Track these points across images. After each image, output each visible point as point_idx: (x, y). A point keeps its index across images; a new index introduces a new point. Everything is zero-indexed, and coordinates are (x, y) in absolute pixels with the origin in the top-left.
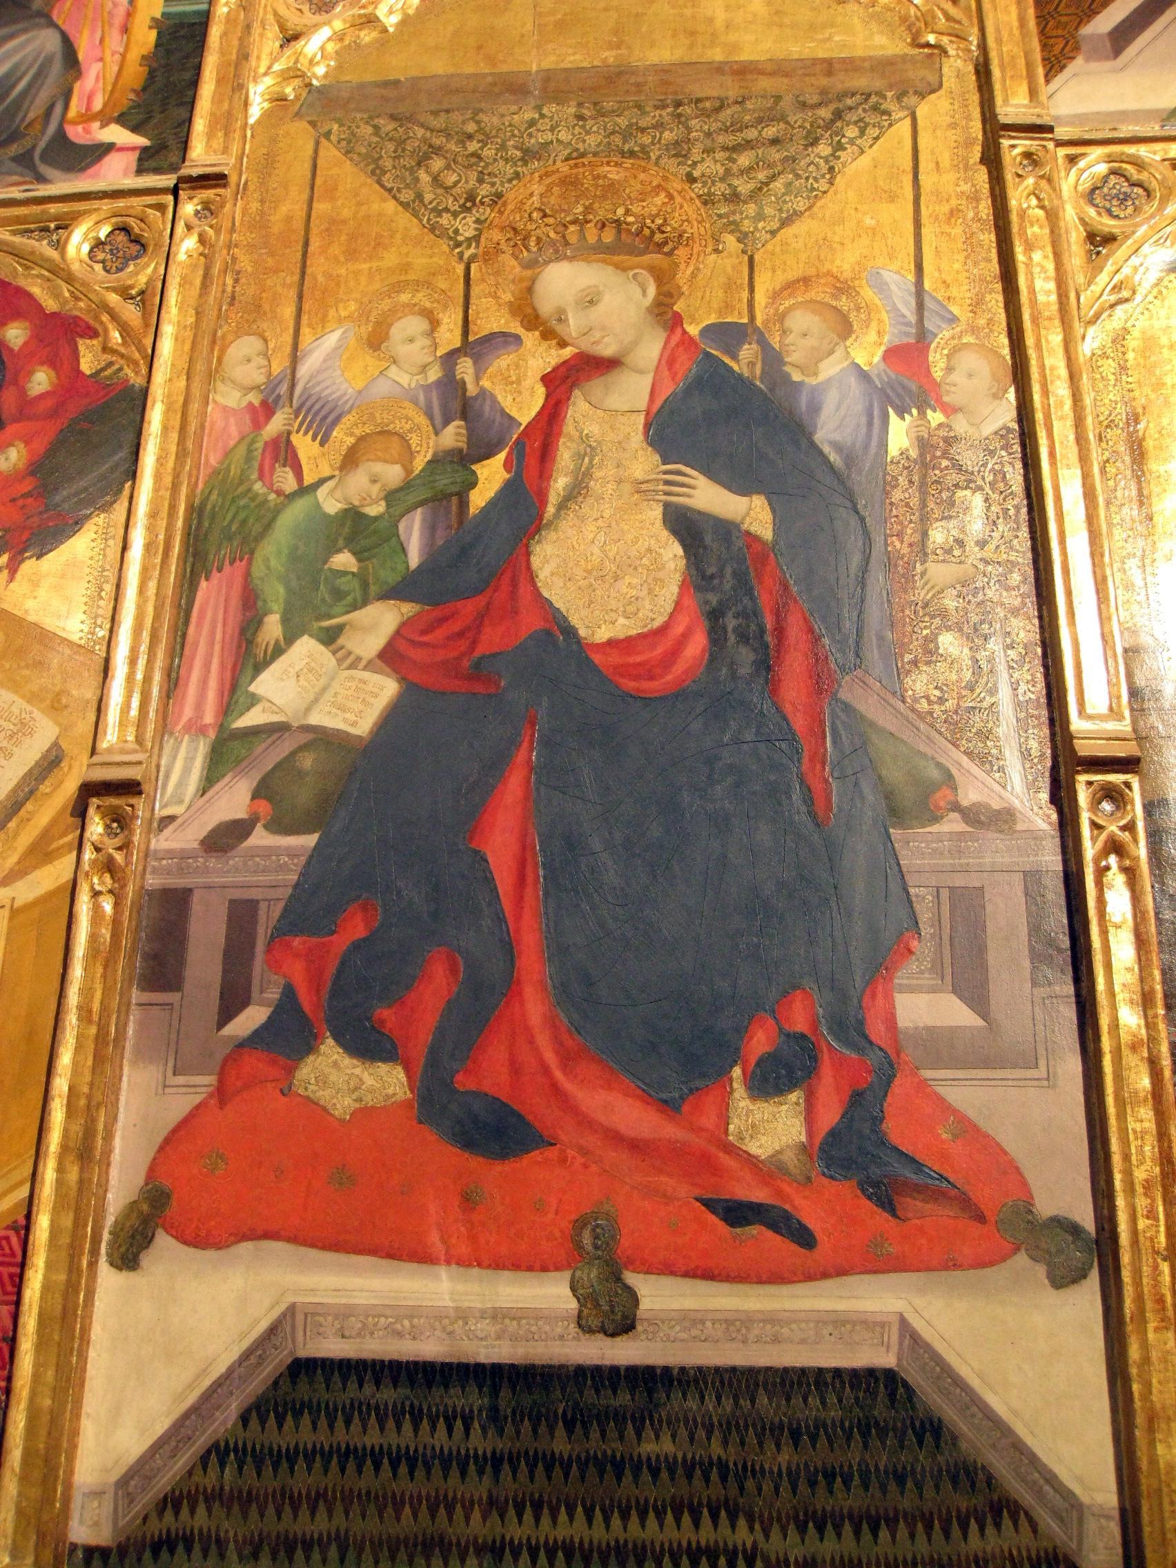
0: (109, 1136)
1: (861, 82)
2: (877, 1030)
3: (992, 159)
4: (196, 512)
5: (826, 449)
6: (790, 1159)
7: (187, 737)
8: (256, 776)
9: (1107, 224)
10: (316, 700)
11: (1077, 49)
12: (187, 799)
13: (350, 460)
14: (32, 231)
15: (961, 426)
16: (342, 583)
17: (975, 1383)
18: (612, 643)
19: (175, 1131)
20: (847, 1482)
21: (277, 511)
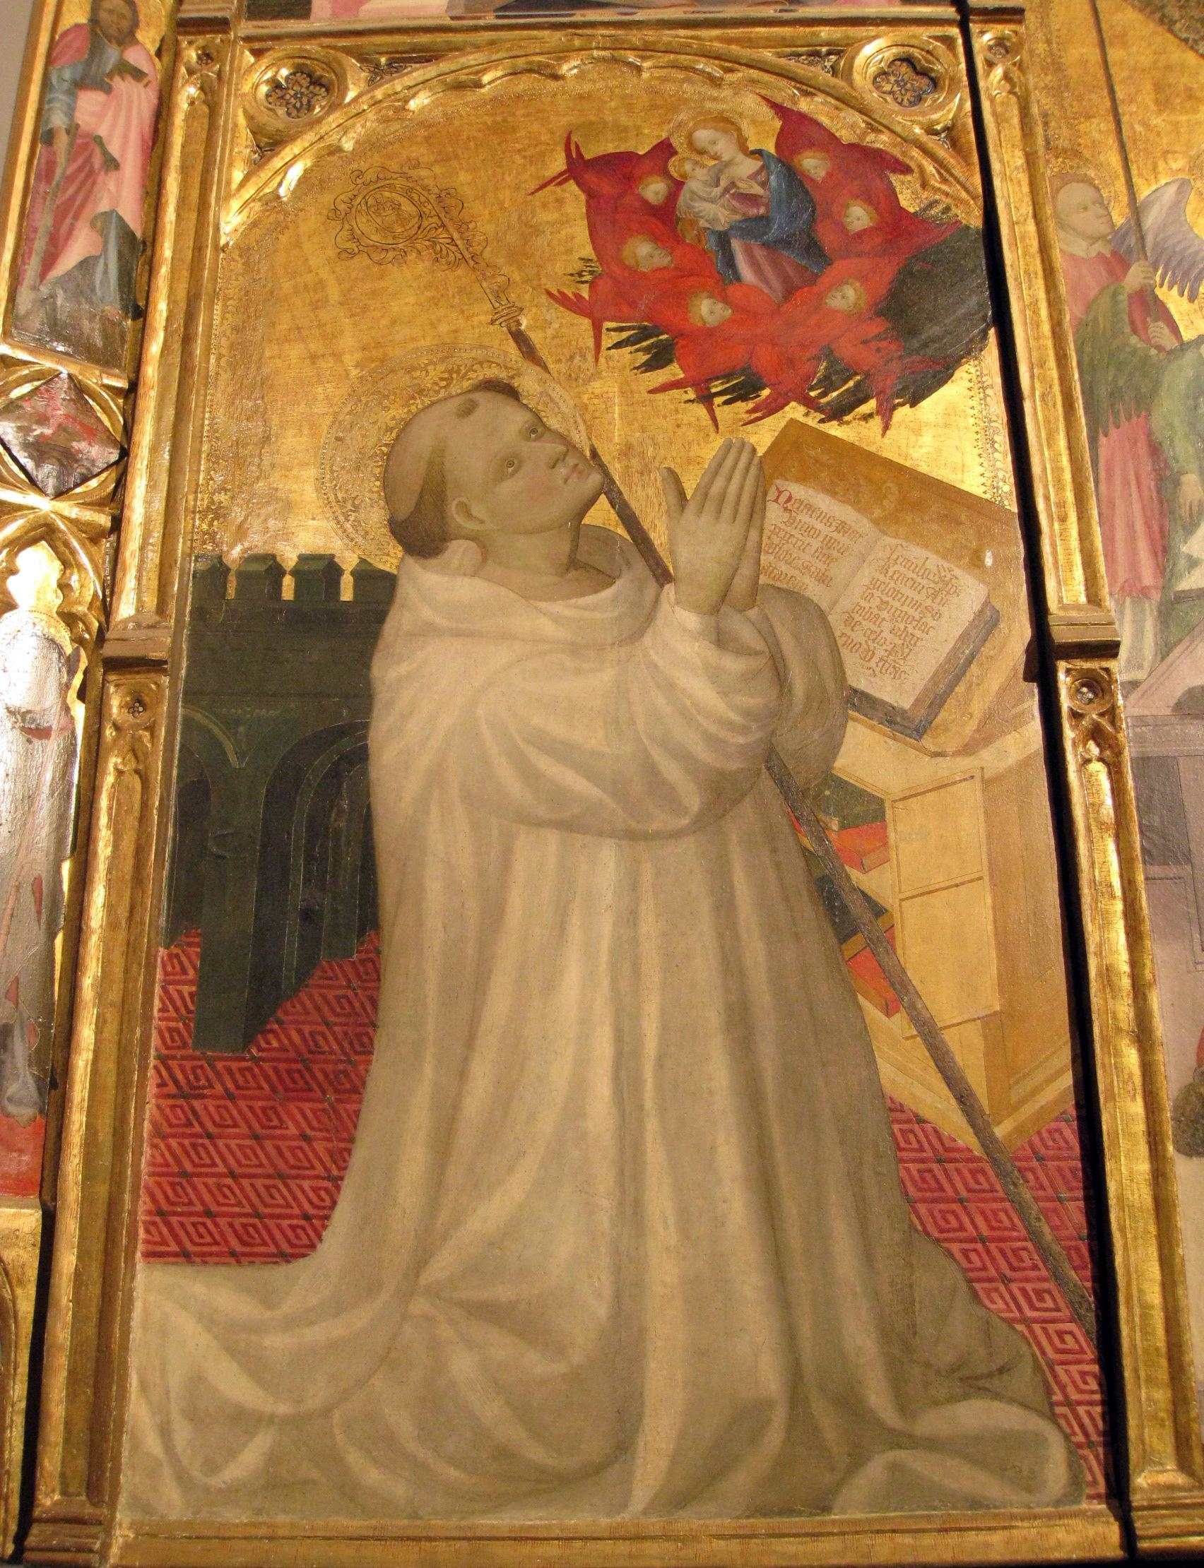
7: (1128, 600)
12: (1147, 665)
14: (800, 55)
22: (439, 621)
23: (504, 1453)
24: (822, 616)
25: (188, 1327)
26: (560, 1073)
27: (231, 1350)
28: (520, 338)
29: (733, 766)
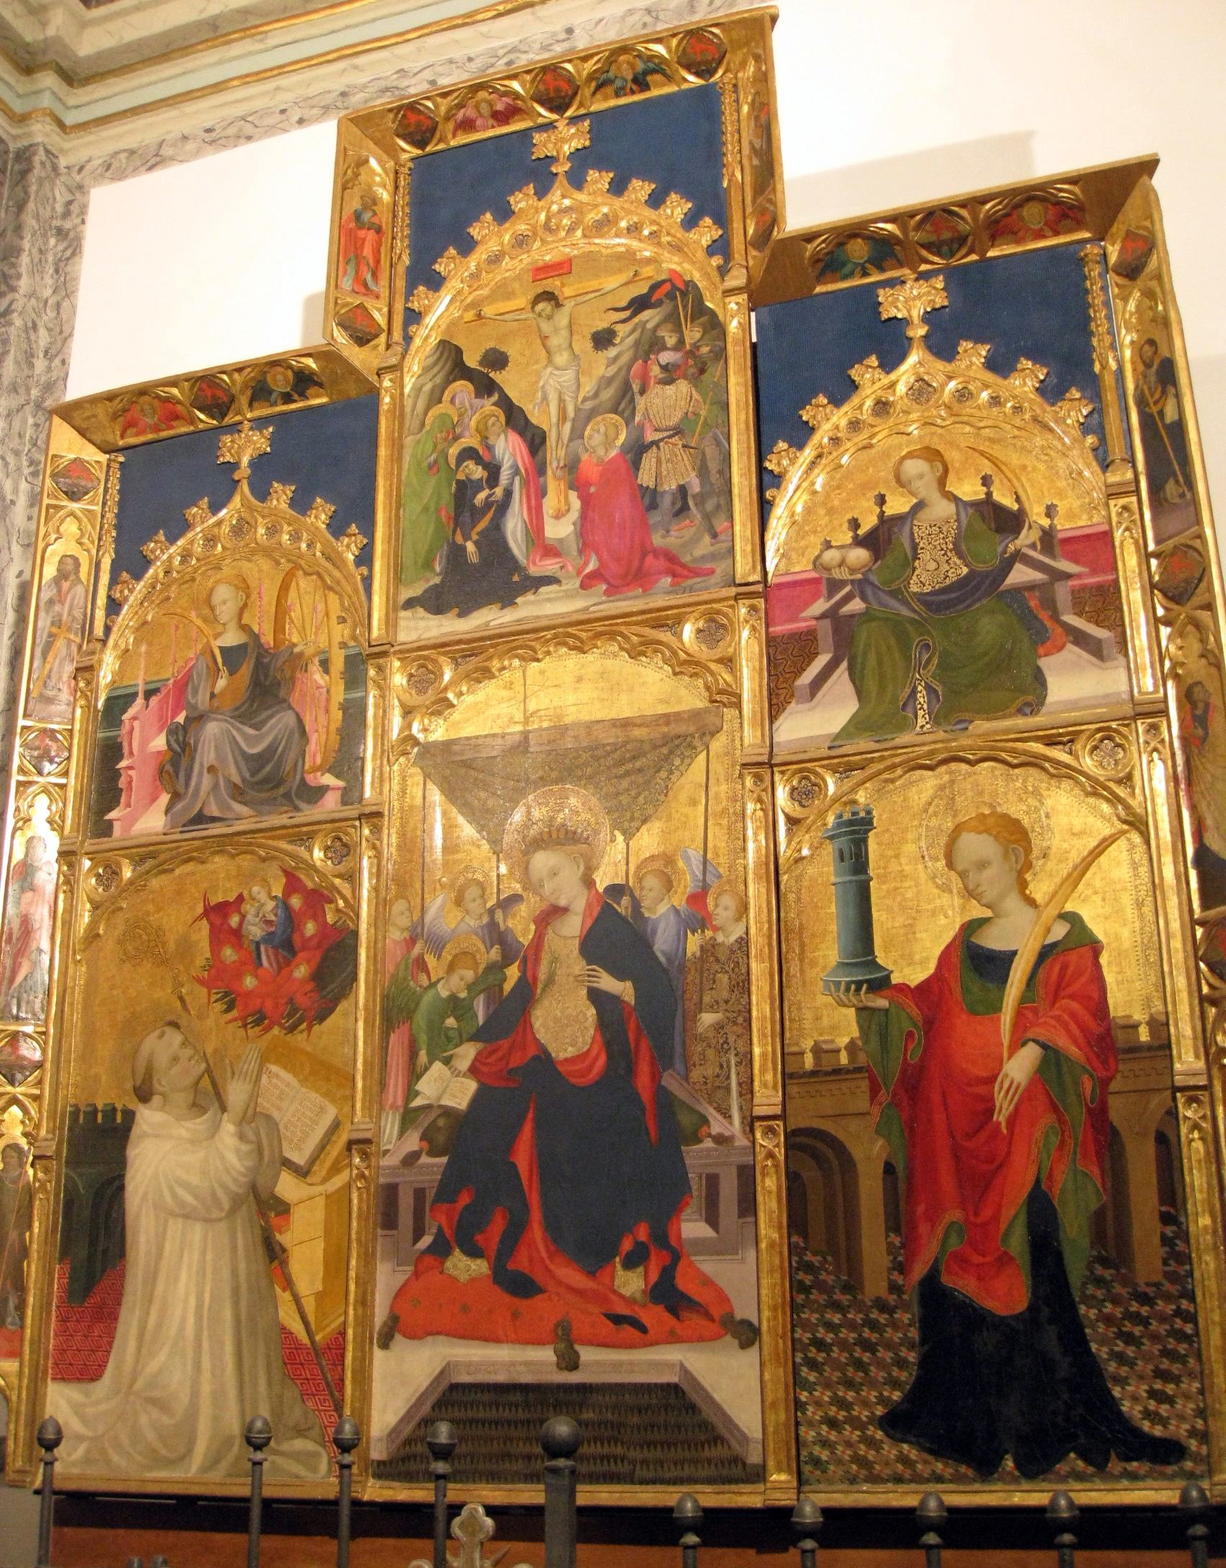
0: (373, 1293)
1: (682, 729)
2: (673, 1242)
4: (385, 997)
5: (659, 954)
6: (638, 1296)
8: (421, 1130)
10: (444, 1092)
11: (792, 695)
13: (451, 968)
15: (720, 938)
16: (451, 1033)
17: (709, 1389)
18: (566, 1060)
19: (400, 1289)
20: (659, 1428)
21: (421, 996)
22: (150, 1131)
23: (154, 1451)
24: (277, 1125)
25: (63, 1404)
26: (178, 1313)
27: (76, 1413)
28: (181, 999)
29: (240, 1191)
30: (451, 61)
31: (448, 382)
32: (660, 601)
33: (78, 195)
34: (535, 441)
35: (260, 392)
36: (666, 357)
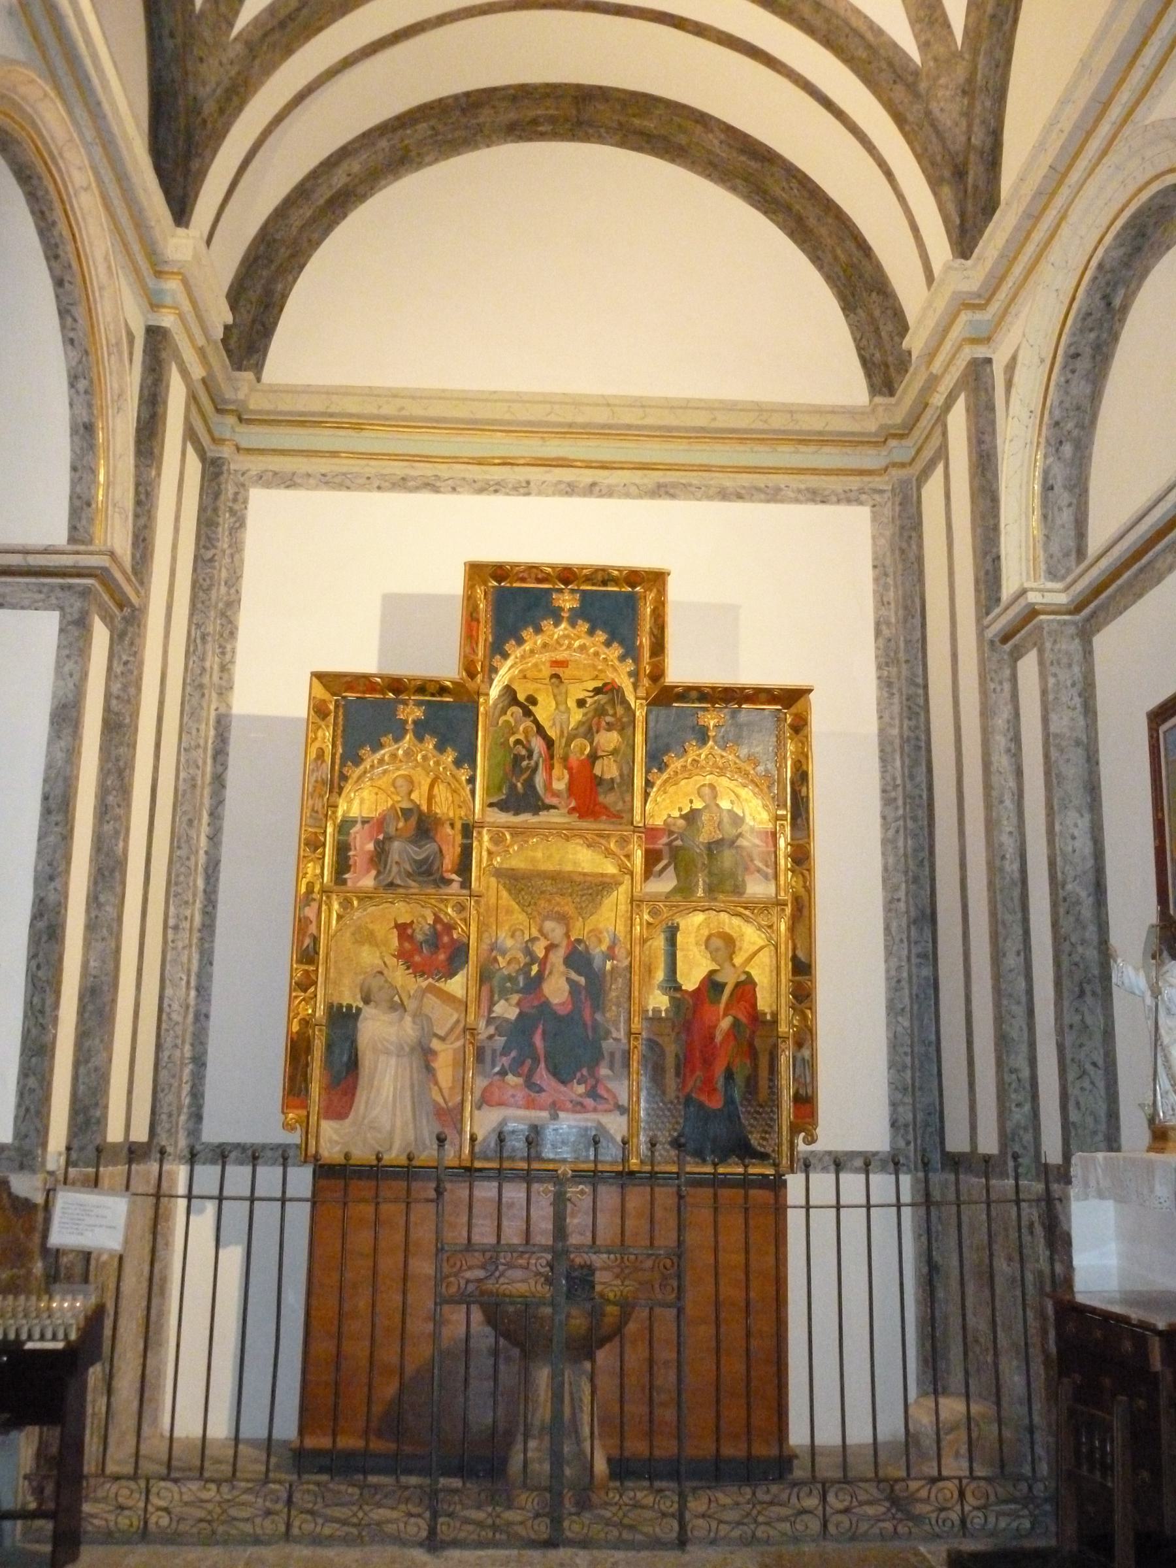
3: (631, 903)
9: (651, 920)
13: (509, 963)
26: (385, 1094)
30: (464, 479)
31: (510, 705)
32: (602, 826)
33: (242, 490)
34: (550, 743)
35: (421, 689)
36: (609, 719)
